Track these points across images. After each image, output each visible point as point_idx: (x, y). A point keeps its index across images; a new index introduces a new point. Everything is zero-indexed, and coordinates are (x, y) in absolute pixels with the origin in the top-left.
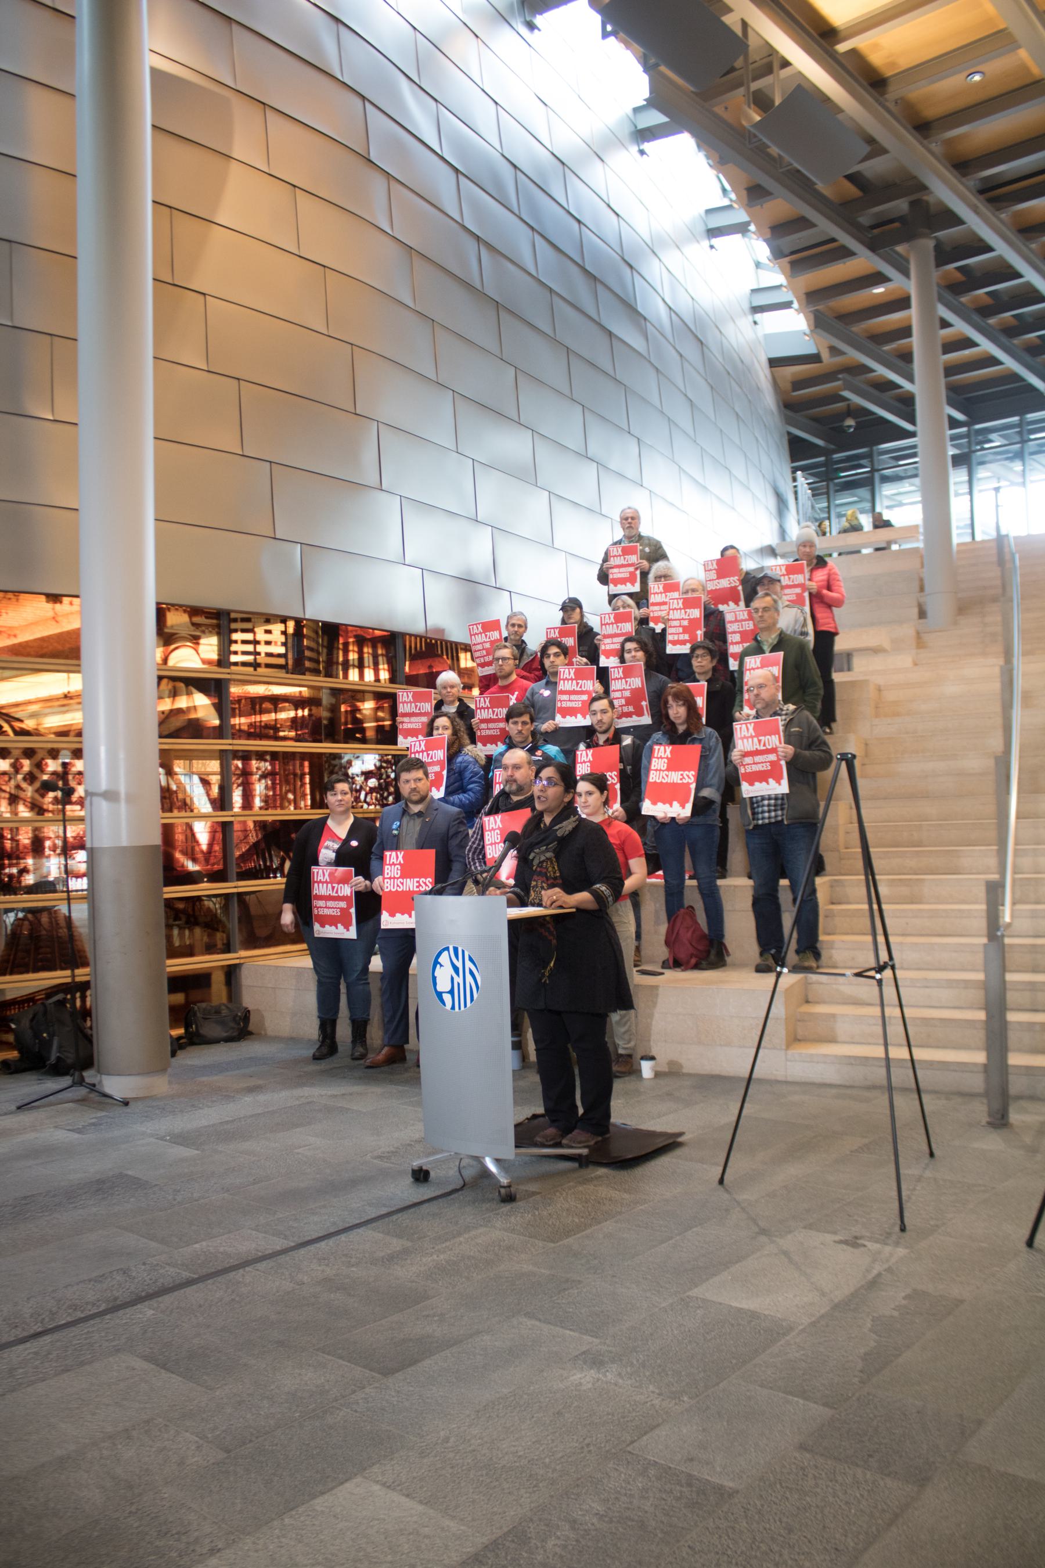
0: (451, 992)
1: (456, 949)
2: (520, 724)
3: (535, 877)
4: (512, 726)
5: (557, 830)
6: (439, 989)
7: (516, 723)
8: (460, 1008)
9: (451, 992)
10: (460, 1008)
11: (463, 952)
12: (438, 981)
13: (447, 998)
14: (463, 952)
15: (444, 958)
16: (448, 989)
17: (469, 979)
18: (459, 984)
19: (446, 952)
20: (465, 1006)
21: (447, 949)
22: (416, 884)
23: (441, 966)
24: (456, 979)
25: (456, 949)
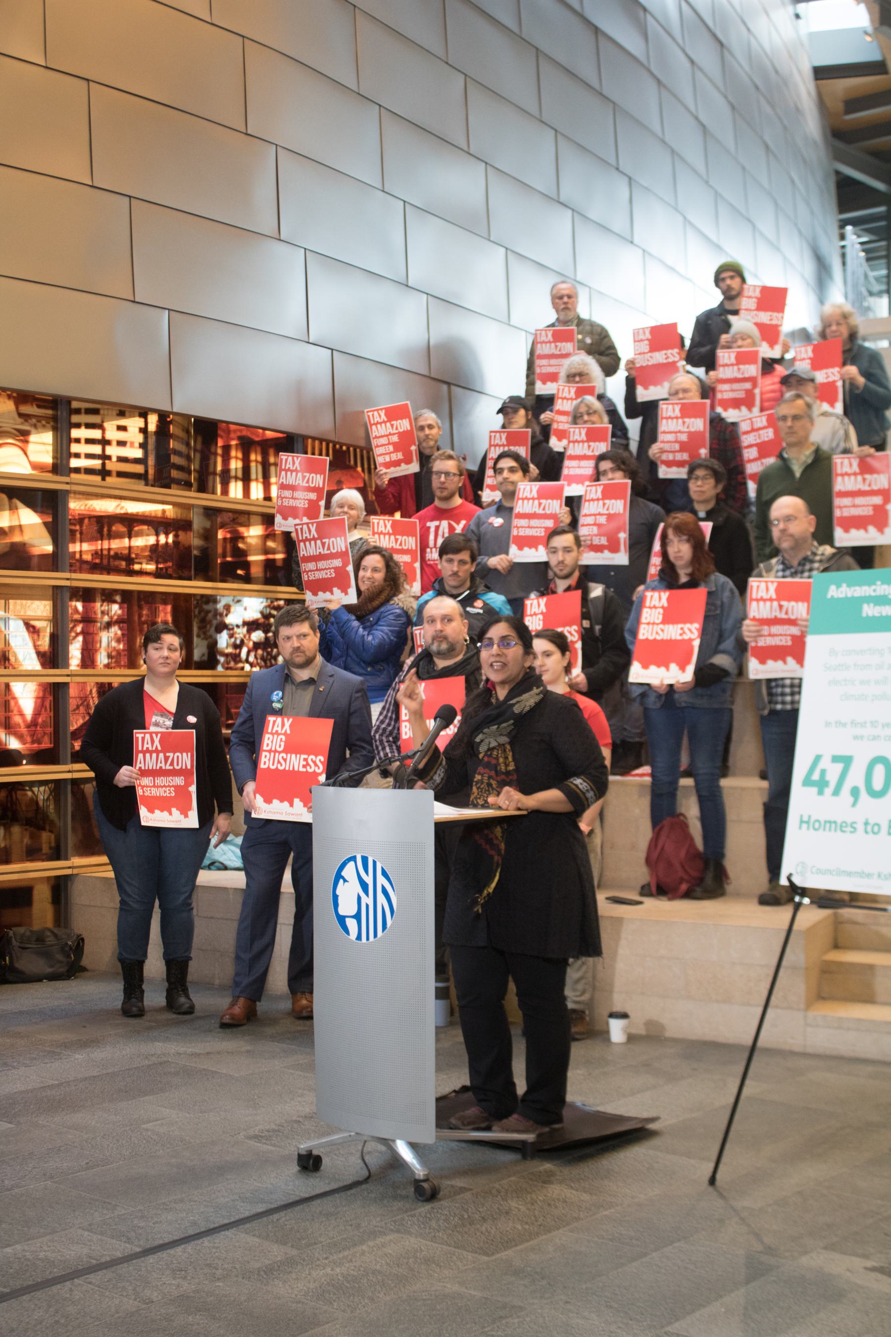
0: (357, 917)
1: (365, 860)
2: (456, 563)
3: (481, 769)
4: (445, 564)
5: (514, 705)
6: (342, 912)
7: (451, 561)
8: (368, 939)
9: (357, 917)
10: (368, 939)
11: (374, 863)
14: (374, 863)
15: (349, 872)
16: (354, 911)
18: (367, 906)
20: (375, 935)
23: (345, 881)
24: (365, 900)
25: (365, 860)
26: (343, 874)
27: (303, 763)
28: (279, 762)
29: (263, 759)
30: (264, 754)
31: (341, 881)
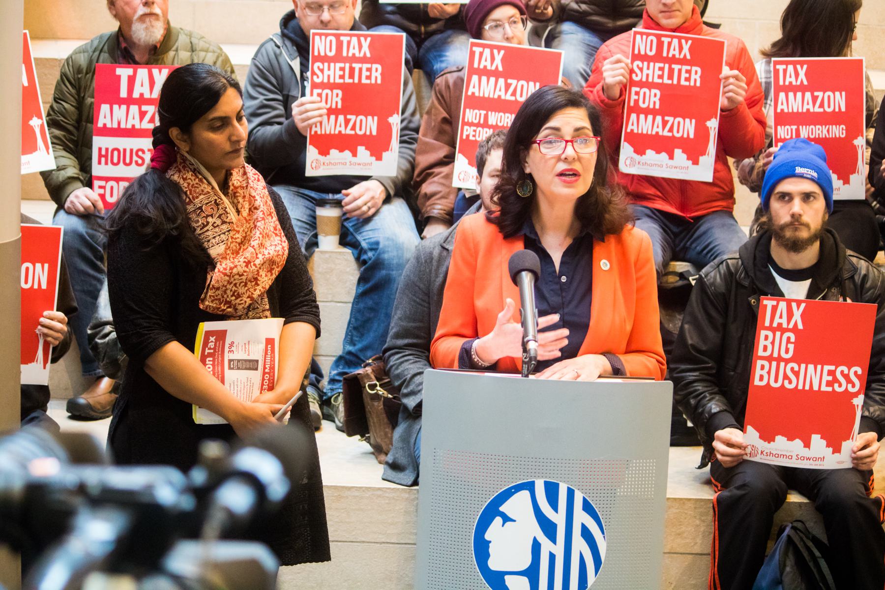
1: (552, 490)
6: (494, 564)
9: (532, 573)
11: (571, 493)
12: (492, 550)
14: (571, 493)
16: (525, 562)
17: (579, 545)
18: (552, 557)
19: (525, 494)
21: (530, 487)
22: (826, 378)
23: (506, 519)
24: (547, 546)
25: (552, 490)
26: (502, 509)
28: (786, 377)
29: (758, 372)
30: (759, 363)
31: (498, 520)
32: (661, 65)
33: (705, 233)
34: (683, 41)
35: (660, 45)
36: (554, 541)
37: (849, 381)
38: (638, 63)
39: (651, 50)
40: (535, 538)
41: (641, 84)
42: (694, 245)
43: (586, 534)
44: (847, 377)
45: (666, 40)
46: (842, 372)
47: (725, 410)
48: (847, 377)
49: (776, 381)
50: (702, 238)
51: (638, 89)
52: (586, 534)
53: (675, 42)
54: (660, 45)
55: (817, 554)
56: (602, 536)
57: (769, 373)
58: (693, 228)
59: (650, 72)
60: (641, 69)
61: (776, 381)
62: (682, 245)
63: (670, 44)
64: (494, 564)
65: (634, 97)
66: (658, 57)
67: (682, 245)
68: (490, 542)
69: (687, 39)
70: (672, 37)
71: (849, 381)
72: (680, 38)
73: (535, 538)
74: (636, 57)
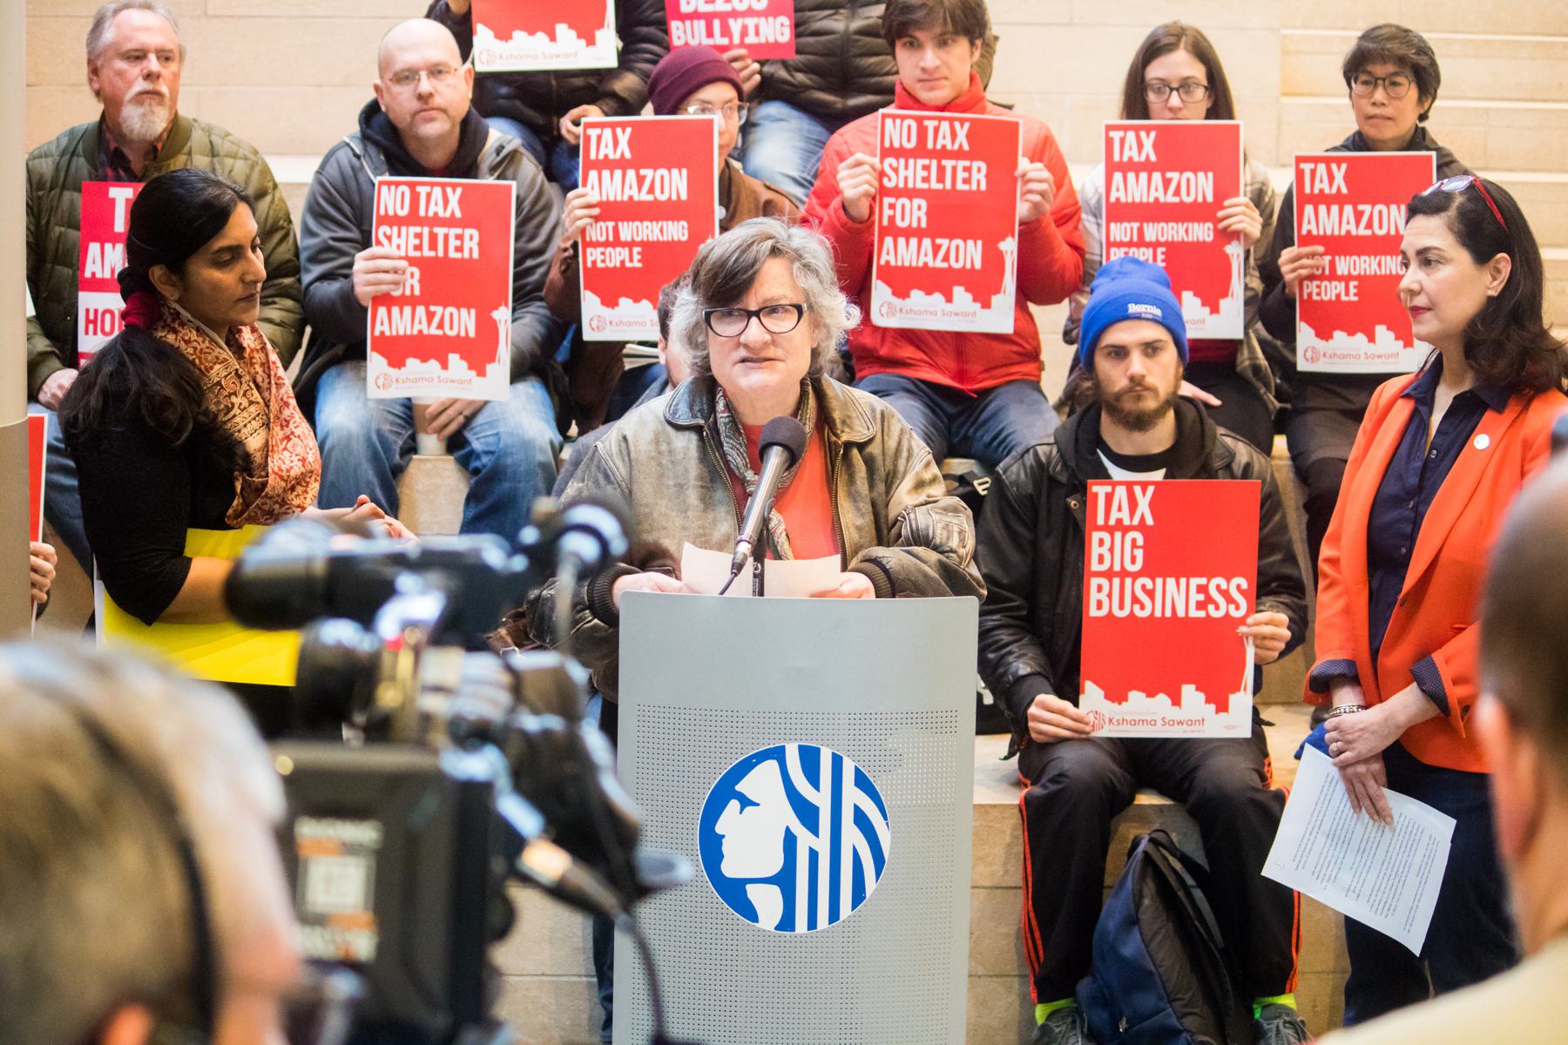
0: (784, 880)
1: (810, 758)
6: (731, 868)
8: (812, 924)
9: (784, 880)
10: (812, 924)
11: (837, 762)
12: (724, 849)
13: (767, 901)
14: (837, 762)
15: (763, 782)
16: (775, 865)
17: (852, 836)
18: (813, 855)
19: (772, 766)
20: (834, 915)
21: (778, 754)
24: (805, 839)
25: (810, 758)
26: (738, 788)
27: (1196, 597)
28: (1135, 600)
29: (1094, 596)
30: (1094, 582)
32: (926, 162)
33: (994, 415)
34: (957, 124)
35: (922, 132)
36: (817, 834)
37: (1230, 600)
38: (890, 161)
39: (909, 140)
40: (788, 829)
41: (897, 193)
42: (979, 434)
43: (861, 819)
44: (1225, 594)
45: (930, 124)
46: (1218, 587)
47: (1039, 674)
48: (1225, 594)
49: (1121, 607)
50: (991, 423)
51: (892, 200)
52: (861, 819)
53: (945, 126)
54: (922, 132)
55: (1190, 881)
56: (884, 822)
57: (1110, 595)
58: (978, 406)
59: (910, 173)
60: (896, 170)
61: (1121, 607)
62: (962, 432)
63: (936, 130)
64: (731, 868)
65: (887, 212)
66: (920, 151)
67: (962, 432)
68: (723, 836)
69: (962, 121)
70: (940, 119)
71: (1230, 600)
72: (951, 120)
73: (788, 829)
74: (887, 152)
